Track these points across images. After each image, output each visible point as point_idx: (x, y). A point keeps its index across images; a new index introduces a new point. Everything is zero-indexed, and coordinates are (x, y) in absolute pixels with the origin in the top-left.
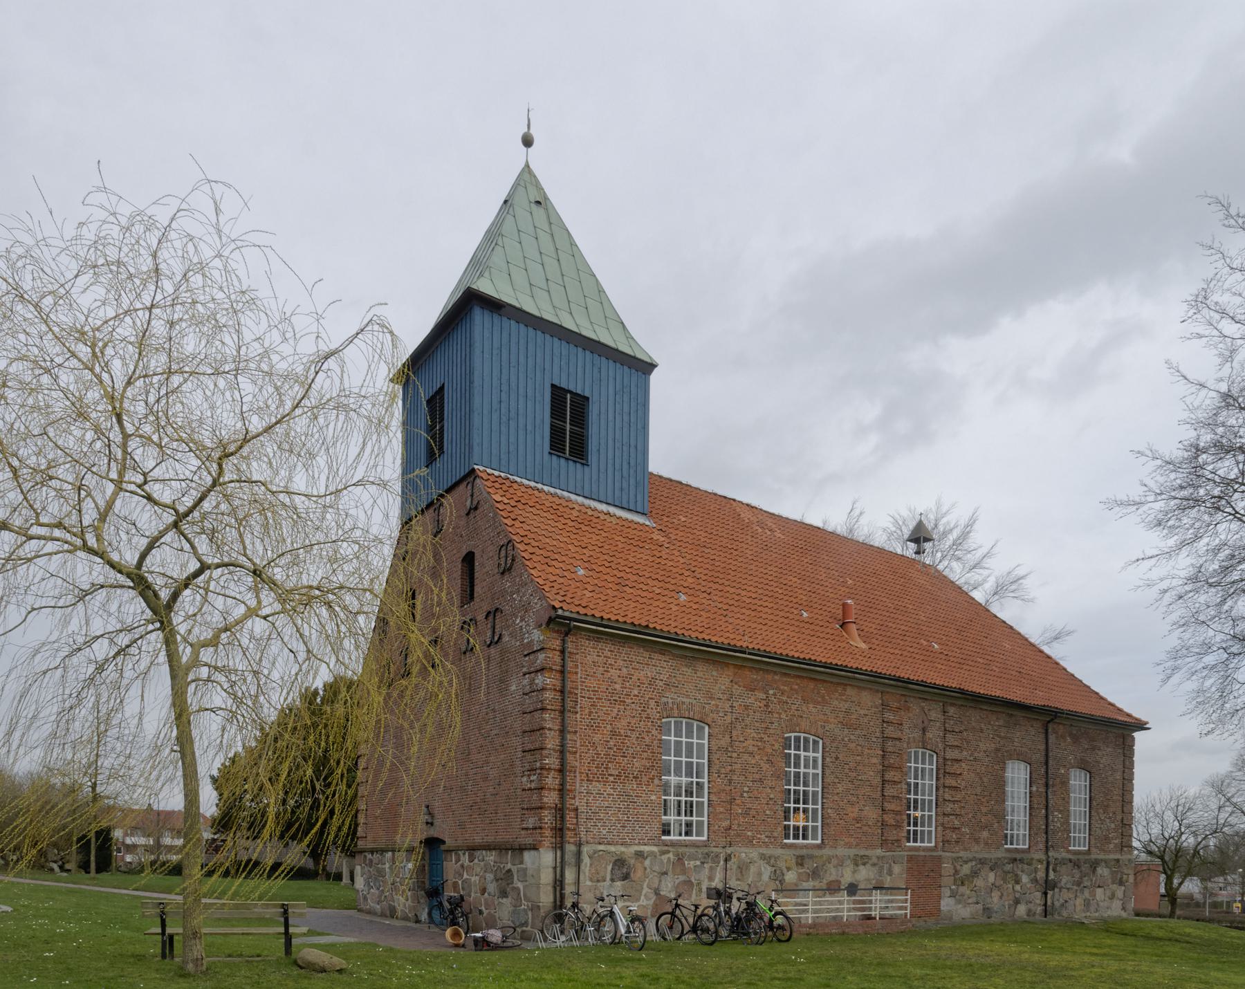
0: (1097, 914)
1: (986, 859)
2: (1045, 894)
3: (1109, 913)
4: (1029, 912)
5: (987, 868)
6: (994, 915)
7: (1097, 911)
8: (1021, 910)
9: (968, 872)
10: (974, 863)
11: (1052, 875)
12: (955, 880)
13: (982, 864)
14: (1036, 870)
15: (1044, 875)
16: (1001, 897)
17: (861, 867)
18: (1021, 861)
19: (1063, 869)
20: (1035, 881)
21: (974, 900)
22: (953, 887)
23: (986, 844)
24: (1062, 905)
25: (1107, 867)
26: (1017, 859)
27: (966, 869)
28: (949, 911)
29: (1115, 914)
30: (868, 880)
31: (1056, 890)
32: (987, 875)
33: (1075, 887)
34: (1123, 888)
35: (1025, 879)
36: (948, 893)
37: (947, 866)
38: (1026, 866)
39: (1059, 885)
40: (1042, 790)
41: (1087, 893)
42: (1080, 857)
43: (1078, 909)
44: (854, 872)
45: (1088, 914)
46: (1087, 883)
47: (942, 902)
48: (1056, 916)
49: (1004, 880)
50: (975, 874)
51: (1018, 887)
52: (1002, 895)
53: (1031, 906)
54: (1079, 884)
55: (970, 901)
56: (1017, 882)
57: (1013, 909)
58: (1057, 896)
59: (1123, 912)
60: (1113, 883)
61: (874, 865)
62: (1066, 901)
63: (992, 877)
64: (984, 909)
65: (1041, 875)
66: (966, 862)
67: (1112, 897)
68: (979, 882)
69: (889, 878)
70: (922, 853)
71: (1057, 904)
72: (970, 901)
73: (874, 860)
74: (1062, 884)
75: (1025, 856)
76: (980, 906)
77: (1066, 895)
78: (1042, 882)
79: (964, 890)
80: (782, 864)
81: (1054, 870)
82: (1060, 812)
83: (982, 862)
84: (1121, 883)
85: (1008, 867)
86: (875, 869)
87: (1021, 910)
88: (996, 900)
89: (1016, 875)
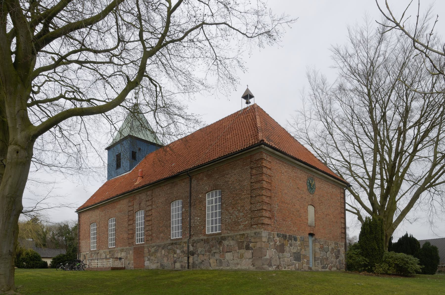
0: (228, 268)
1: (160, 245)
2: (188, 258)
3: (239, 267)
4: (182, 266)
5: (160, 249)
6: (165, 267)
7: (228, 266)
8: (178, 265)
9: (154, 251)
10: (155, 247)
11: (191, 249)
12: (149, 254)
13: (159, 247)
14: (183, 247)
15: (187, 249)
16: (168, 260)
17: (122, 252)
18: (176, 244)
19: (199, 244)
20: (183, 252)
21: (156, 261)
22: (149, 257)
23: (162, 239)
24: (201, 263)
25: (233, 240)
26: (175, 243)
27: (153, 250)
28: (148, 266)
29: (244, 267)
30: (124, 256)
31: (195, 255)
32: (161, 251)
33: (208, 253)
34: (251, 251)
35: (178, 251)
36: (147, 260)
37: (146, 250)
38: (178, 246)
39: (197, 253)
40: (188, 209)
41: (217, 256)
42: (210, 237)
43: (212, 265)
44: (121, 254)
45: (221, 268)
46: (215, 251)
47: (145, 263)
48: (198, 268)
49: (168, 252)
50: (156, 251)
51: (175, 256)
52: (168, 259)
53: (183, 264)
54: (210, 252)
55: (155, 262)
56: (175, 253)
57: (173, 265)
58: (196, 259)
59: (251, 267)
60: (240, 249)
61: (125, 251)
62: (203, 261)
63: (163, 252)
64: (161, 265)
65: (185, 249)
66: (153, 247)
67: (242, 257)
68: (159, 255)
69: (129, 255)
70: (139, 246)
71: (197, 262)
72: (155, 262)
73: (125, 250)
74: (199, 252)
75: (178, 241)
76: (159, 264)
77: (201, 258)
78: (187, 252)
79: (152, 258)
80: (107, 254)
81: (193, 246)
82: (198, 216)
83: (159, 246)
84: (248, 248)
85: (169, 247)
86: (125, 253)
87: (178, 265)
88: (165, 261)
89: (174, 250)
